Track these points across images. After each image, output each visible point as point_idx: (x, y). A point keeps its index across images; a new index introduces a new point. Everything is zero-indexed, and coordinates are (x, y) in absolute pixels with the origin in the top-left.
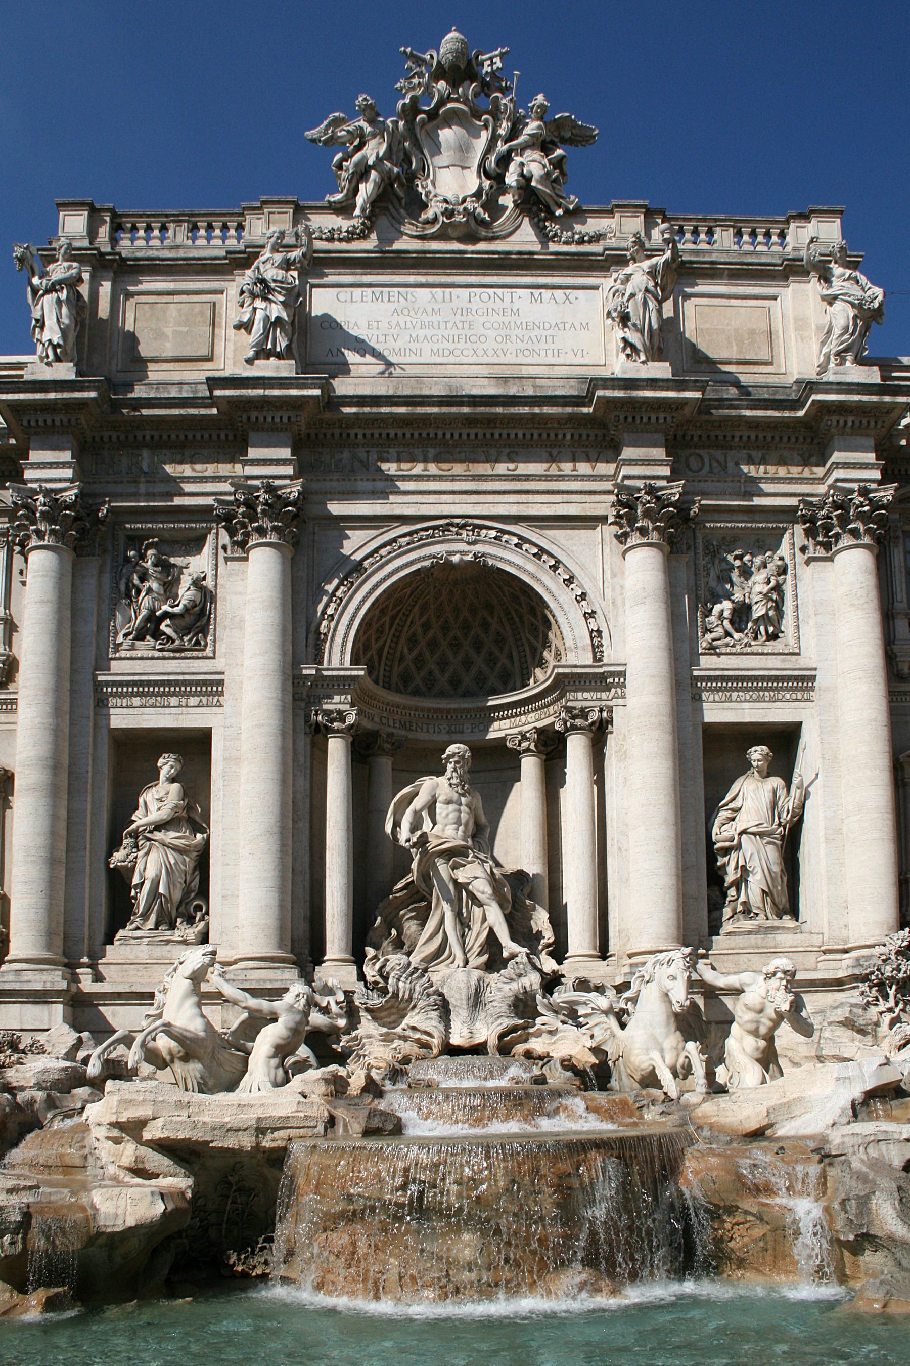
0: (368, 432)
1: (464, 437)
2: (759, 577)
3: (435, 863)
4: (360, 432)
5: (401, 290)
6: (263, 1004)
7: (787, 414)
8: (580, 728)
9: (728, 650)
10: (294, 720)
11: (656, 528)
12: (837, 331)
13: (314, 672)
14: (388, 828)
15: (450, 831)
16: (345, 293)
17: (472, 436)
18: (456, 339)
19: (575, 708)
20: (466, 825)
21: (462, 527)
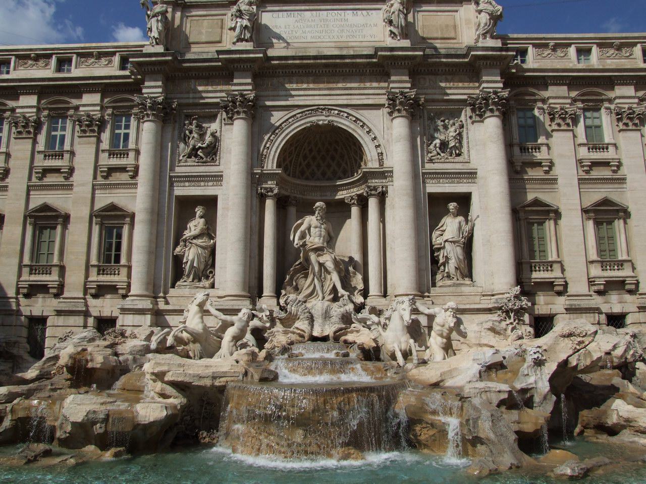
0: (284, 71)
1: (324, 72)
2: (452, 129)
4: (281, 71)
5: (299, 12)
6: (228, 318)
7: (461, 60)
8: (374, 195)
9: (436, 161)
10: (251, 192)
11: (405, 109)
12: (482, 25)
15: (317, 240)
16: (275, 14)
17: (327, 71)
18: (321, 32)
20: (324, 237)
21: (324, 109)
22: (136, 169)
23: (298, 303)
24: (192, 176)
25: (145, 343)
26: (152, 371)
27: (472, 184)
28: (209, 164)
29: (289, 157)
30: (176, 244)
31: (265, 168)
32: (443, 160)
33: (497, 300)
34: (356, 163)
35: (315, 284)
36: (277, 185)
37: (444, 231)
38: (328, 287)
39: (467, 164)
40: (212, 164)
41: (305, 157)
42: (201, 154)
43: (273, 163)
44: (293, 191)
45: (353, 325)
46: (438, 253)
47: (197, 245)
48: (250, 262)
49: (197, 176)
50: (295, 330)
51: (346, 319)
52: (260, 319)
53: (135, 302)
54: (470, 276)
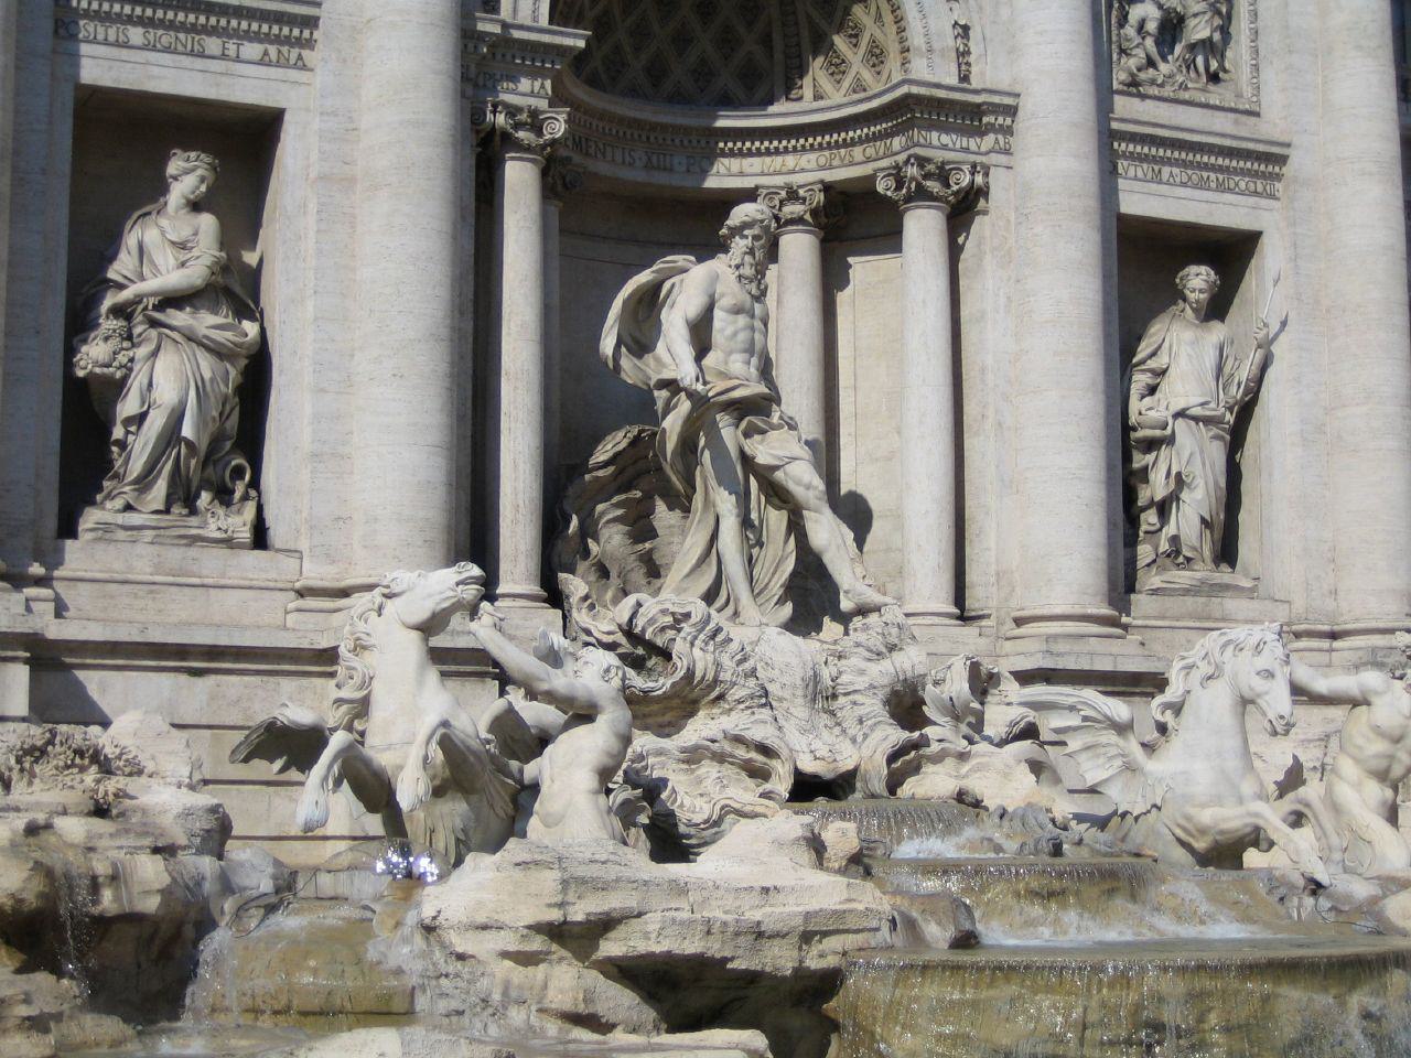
3: (715, 423)
9: (1154, 91)
13: (497, 29)
15: (737, 365)
19: (929, 160)
23: (713, 637)
26: (555, 915)
27: (1264, 202)
30: (79, 324)
32: (1167, 92)
33: (1374, 650)
37: (1163, 372)
39: (1253, 120)
45: (928, 730)
46: (1150, 458)
47: (191, 338)
50: (727, 747)
51: (907, 706)
54: (1226, 552)
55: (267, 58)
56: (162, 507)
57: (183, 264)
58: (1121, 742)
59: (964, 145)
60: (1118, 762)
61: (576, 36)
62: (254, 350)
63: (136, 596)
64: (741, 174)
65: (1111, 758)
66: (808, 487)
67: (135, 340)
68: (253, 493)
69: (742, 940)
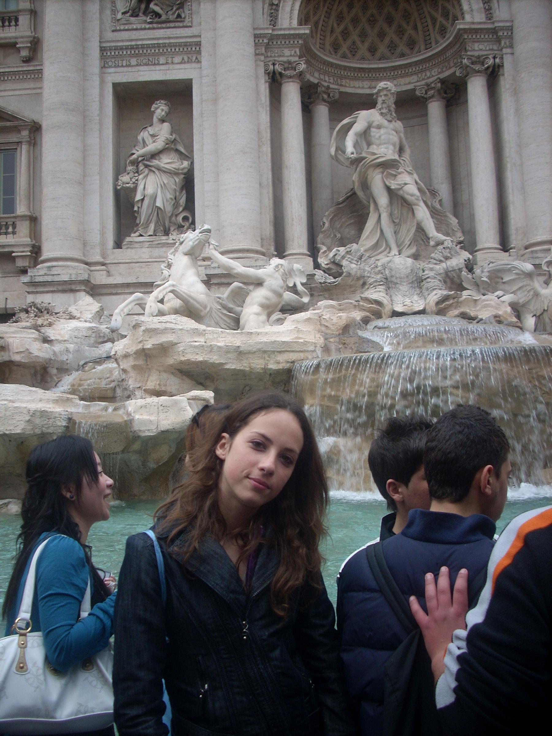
8: (479, 72)
10: (256, 70)
13: (270, 32)
14: (333, 151)
20: (394, 145)
22: (35, 45)
23: (360, 258)
24: (143, 47)
25: (93, 325)
26: (140, 346)
28: (172, 25)
29: (314, 15)
31: (279, 26)
34: (434, 24)
35: (382, 231)
36: (300, 57)
38: (408, 233)
40: (177, 24)
41: (340, 18)
42: (157, 9)
43: (291, 18)
44: (322, 77)
45: (465, 293)
47: (159, 169)
48: (261, 194)
49: (153, 46)
51: (454, 282)
52: (294, 289)
53: (55, 271)
55: (183, 61)
56: (152, 234)
57: (154, 142)
58: (531, 284)
59: (491, 48)
60: (532, 293)
61: (304, 29)
62: (186, 171)
63: (142, 267)
64: (409, 83)
65: (529, 292)
66: (412, 195)
67: (140, 173)
68: (193, 226)
69: (229, 355)
